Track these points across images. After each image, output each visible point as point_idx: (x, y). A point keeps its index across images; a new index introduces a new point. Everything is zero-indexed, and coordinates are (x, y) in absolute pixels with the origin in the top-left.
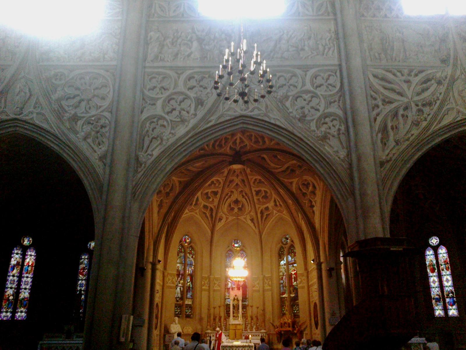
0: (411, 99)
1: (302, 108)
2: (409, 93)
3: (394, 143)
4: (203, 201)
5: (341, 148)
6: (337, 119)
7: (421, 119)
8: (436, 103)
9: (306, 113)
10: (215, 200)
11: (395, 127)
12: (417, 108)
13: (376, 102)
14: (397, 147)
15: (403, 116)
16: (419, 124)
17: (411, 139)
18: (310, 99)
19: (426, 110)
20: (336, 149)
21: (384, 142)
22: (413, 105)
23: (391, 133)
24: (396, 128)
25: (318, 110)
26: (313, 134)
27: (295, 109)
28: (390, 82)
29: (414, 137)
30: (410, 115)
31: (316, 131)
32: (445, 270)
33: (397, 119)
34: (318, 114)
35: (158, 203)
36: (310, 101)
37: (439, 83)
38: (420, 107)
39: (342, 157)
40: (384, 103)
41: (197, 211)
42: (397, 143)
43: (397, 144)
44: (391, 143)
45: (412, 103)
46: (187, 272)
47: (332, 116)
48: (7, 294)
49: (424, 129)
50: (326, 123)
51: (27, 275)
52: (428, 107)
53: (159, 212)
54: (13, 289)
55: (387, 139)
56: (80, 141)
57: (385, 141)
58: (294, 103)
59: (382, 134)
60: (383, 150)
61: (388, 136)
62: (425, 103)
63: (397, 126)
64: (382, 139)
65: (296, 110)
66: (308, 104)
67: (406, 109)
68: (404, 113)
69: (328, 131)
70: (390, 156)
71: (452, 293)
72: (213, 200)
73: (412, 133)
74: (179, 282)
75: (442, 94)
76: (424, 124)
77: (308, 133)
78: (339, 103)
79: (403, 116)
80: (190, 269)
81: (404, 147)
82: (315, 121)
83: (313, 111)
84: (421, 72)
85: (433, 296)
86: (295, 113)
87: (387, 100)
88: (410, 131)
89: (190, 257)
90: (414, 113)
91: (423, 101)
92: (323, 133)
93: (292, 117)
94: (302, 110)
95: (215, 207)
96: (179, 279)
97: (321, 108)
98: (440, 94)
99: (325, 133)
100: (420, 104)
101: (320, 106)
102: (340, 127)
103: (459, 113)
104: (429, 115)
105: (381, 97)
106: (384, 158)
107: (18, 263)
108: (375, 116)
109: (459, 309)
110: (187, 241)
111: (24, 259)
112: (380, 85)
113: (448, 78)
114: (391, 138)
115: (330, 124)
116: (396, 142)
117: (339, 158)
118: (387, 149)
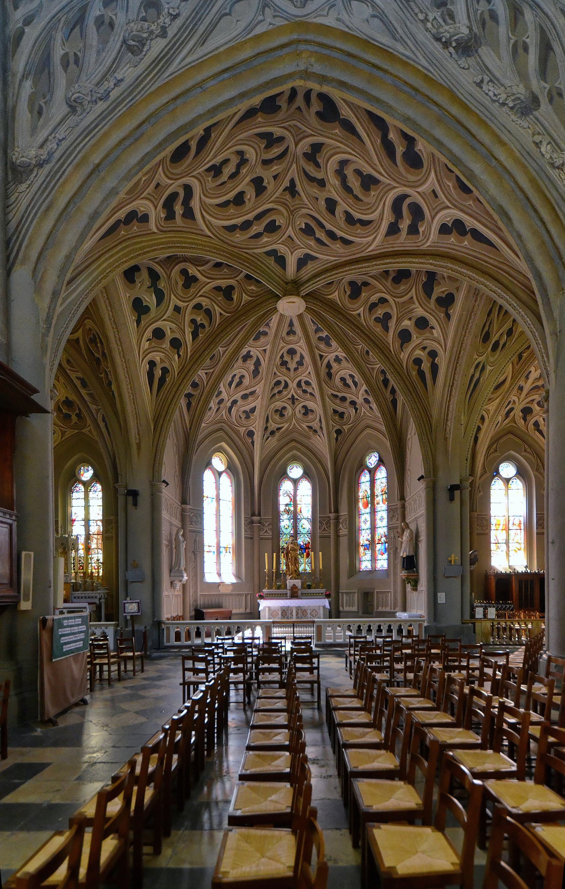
3: (65, 109)
7: (151, 32)
11: (72, 59)
15: (100, 22)
16: (143, 45)
17: (114, 95)
24: (76, 62)
29: (123, 86)
30: (120, 19)
33: (83, 35)
43: (73, 109)
49: (156, 61)
55: (48, 97)
57: (42, 103)
59: (35, 84)
60: (34, 130)
61: (51, 90)
68: (103, 11)
70: (51, 145)
73: (119, 77)
79: (100, 22)
81: (91, 118)
103: (267, 9)
106: (33, 153)
108: (20, 25)
114: (60, 94)
116: (70, 106)
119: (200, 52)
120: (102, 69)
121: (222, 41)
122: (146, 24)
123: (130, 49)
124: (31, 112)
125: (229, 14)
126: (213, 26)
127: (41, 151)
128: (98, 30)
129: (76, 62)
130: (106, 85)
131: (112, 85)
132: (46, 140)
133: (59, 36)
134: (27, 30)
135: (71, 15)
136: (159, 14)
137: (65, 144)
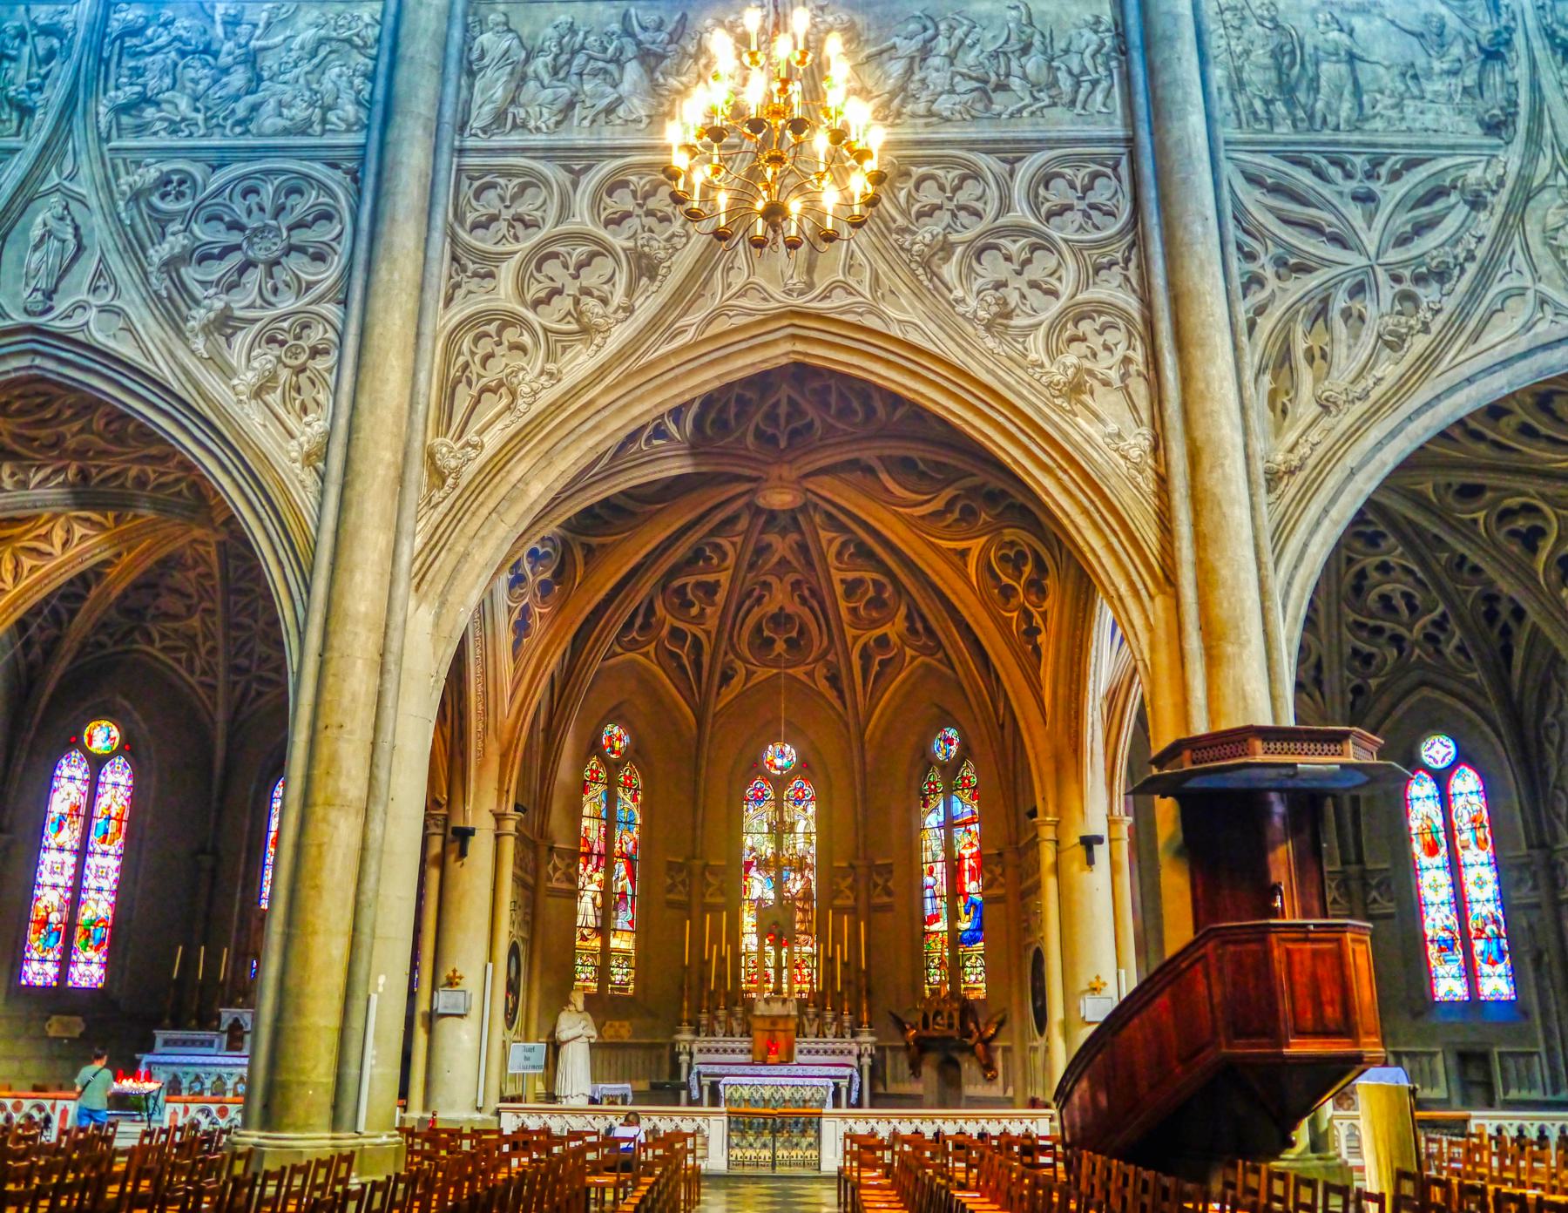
0: (1378, 257)
1: (1000, 285)
2: (1370, 240)
3: (1316, 409)
4: (669, 617)
5: (1133, 425)
6: (1121, 324)
7: (1411, 328)
8: (1463, 271)
9: (1013, 305)
10: (709, 610)
11: (1317, 353)
12: (1398, 288)
13: (1253, 267)
14: (1326, 422)
15: (1346, 314)
17: (1374, 395)
18: (1024, 256)
19: (1429, 294)
20: (1113, 427)
21: (1279, 406)
22: (1382, 276)
23: (1306, 375)
24: (1324, 356)
25: (1054, 293)
26: (1037, 376)
27: (975, 288)
28: (1305, 202)
30: (1371, 311)
31: (1047, 363)
32: (1473, 846)
33: (1328, 328)
34: (1056, 306)
35: (515, 615)
36: (1028, 261)
37: (1476, 203)
38: (1407, 286)
39: (1134, 453)
40: (1282, 271)
41: (651, 648)
42: (1326, 406)
43: (1326, 409)
44: (1305, 408)
45: (1378, 270)
46: (617, 845)
47: (1100, 313)
48: (40, 905)
49: (1422, 359)
50: (1084, 339)
51: (105, 847)
52: (1435, 286)
53: (517, 644)
54: (61, 890)
55: (1292, 394)
56: (240, 401)
57: (1285, 400)
58: (970, 267)
59: (1275, 378)
60: (1278, 432)
61: (1294, 385)
62: (1424, 269)
63: (1327, 349)
64: (1273, 396)
65: (979, 293)
66: (1019, 273)
67: (1358, 290)
68: (1349, 303)
69: (1088, 364)
70: (1303, 450)
71: (1496, 922)
72: (703, 610)
73: (1379, 374)
74: (590, 877)
75: (1487, 242)
76: (1420, 343)
77: (1019, 372)
78: (1126, 268)
80: (626, 838)
82: (1042, 330)
83: (1035, 297)
84: (1411, 164)
85: (1430, 933)
86: (972, 302)
87: (1292, 261)
88: (1372, 368)
89: (627, 798)
90: (1386, 305)
91: (1419, 266)
92: (1070, 372)
93: (963, 316)
94: (998, 294)
95: (708, 633)
96: (590, 868)
97: (1065, 289)
98: (1480, 239)
99: (1078, 369)
100: (1407, 273)
101: (1060, 279)
102: (1130, 353)
103: (1546, 307)
104: (1438, 311)
105: (1273, 250)
106: (1280, 458)
107: (75, 809)
109: (1516, 976)
110: (617, 745)
111: (93, 795)
112: (1271, 209)
113: (1509, 183)
115: (1096, 342)
117: (1125, 457)
118: (1291, 427)
119: (1472, 350)
120: (1355, 367)
121: (1497, 339)
122: (1403, 319)
123: (1387, 344)
124: (1273, 409)
125: (1502, 310)
126: (1485, 323)
127: (1291, 456)
128: (1346, 322)
129: (1324, 356)
130: (1363, 384)
131: (1371, 382)
132: (1296, 443)
133: (1299, 329)
134: (1259, 320)
135: (1311, 306)
136: (1417, 308)
137: (1320, 450)
